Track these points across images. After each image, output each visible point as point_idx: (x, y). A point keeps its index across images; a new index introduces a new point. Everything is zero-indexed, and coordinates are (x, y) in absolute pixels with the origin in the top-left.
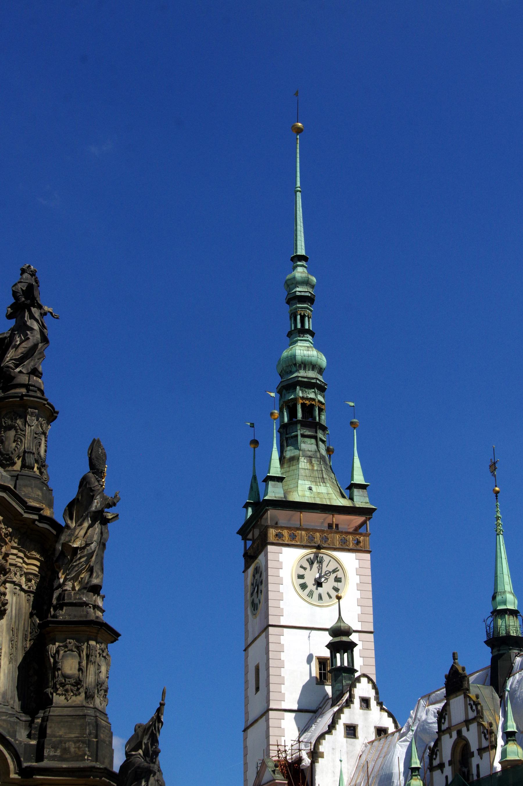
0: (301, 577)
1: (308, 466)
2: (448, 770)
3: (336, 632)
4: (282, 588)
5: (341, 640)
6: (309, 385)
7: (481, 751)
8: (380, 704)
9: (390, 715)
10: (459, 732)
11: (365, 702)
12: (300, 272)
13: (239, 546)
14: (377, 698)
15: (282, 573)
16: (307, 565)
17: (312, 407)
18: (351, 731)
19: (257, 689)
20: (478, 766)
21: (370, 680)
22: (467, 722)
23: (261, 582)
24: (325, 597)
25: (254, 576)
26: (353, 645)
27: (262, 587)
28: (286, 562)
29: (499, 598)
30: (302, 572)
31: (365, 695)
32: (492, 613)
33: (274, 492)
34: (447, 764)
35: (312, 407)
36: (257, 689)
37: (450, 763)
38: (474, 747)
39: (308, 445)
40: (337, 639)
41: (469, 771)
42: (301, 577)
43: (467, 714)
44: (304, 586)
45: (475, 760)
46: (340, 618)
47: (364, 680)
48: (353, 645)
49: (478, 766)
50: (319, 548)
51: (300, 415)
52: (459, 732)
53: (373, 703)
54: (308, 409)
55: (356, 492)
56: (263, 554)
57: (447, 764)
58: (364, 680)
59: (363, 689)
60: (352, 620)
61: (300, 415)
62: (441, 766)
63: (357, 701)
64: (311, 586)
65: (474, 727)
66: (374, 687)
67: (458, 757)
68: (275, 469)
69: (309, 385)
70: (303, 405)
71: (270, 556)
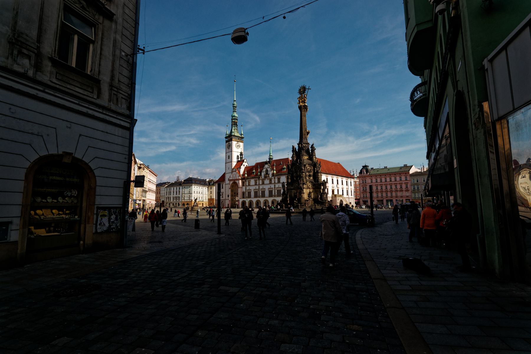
5: (241, 154)
28: (234, 143)
33: (233, 134)
59: (245, 161)
60: (243, 152)
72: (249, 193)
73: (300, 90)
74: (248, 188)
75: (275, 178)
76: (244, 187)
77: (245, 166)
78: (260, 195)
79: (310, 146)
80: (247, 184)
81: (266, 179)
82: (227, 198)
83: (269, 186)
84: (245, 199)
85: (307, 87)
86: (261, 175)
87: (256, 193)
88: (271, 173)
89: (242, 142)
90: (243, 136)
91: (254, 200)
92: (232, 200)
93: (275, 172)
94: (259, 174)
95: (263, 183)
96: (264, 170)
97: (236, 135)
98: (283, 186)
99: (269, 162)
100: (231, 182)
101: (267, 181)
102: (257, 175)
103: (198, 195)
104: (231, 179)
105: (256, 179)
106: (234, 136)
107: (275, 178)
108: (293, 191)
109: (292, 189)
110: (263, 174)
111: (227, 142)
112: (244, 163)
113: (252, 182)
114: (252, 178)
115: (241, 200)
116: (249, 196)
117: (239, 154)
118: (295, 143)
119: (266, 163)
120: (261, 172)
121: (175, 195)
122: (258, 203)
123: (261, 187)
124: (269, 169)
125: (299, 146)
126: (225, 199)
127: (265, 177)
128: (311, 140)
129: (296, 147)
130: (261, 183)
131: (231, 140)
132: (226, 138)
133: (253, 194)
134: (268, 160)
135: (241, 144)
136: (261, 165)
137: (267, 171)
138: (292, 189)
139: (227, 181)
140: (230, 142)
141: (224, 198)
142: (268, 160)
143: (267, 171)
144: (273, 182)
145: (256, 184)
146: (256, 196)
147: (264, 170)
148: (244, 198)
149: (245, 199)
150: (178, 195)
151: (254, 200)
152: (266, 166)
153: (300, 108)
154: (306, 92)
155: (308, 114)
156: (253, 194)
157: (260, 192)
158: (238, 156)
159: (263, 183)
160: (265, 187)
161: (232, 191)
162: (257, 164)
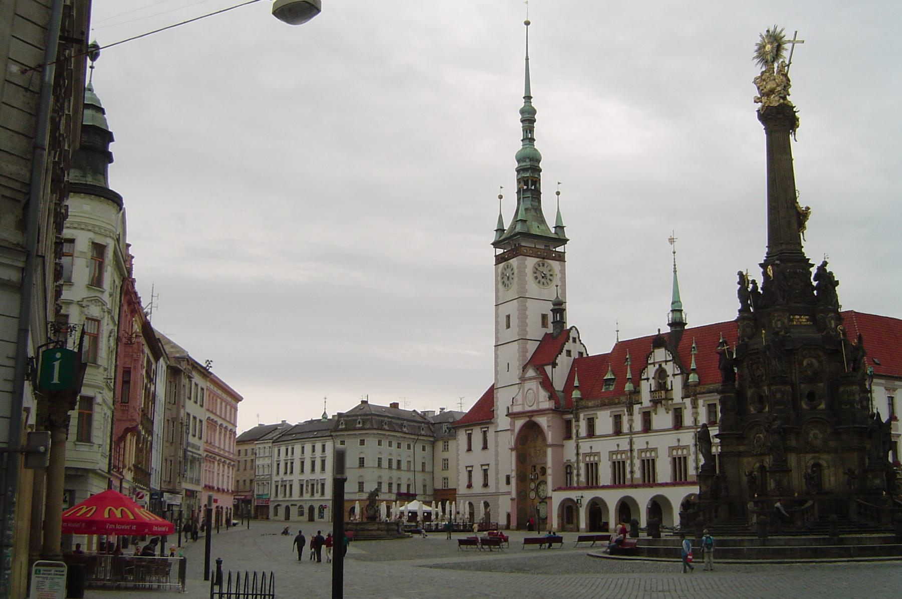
2: (652, 381)
7: (674, 375)
10: (660, 366)
11: (574, 340)
18: (569, 353)
19: (508, 326)
22: (666, 361)
36: (508, 326)
40: (556, 307)
41: (665, 383)
44: (536, 278)
45: (669, 379)
52: (660, 366)
59: (573, 334)
62: (648, 379)
63: (571, 339)
64: (540, 278)
72: (592, 469)
73: (761, 47)
74: (585, 447)
75: (695, 406)
76: (570, 445)
77: (575, 355)
78: (638, 474)
79: (813, 271)
80: (583, 431)
81: (661, 410)
82: (503, 488)
83: (671, 439)
84: (573, 495)
85: (788, 36)
86: (637, 392)
87: (618, 468)
88: (676, 384)
91: (612, 499)
92: (522, 495)
95: (647, 427)
96: (651, 371)
98: (703, 438)
100: (519, 423)
101: (662, 419)
102: (620, 391)
103: (395, 474)
104: (517, 409)
105: (617, 410)
107: (695, 406)
108: (745, 460)
109: (740, 454)
110: (646, 388)
111: (499, 259)
112: (569, 346)
113: (604, 421)
114: (603, 406)
115: (558, 498)
116: (592, 482)
117: (547, 308)
118: (751, 255)
119: (658, 341)
120: (636, 381)
121: (308, 475)
122: (626, 508)
123: (640, 442)
124: (670, 368)
125: (765, 274)
126: (497, 494)
127: (656, 402)
128: (815, 247)
129: (757, 277)
130: (638, 425)
132: (496, 244)
133: (605, 475)
134: (668, 330)
136: (634, 353)
137: (661, 373)
138: (740, 454)
139: (502, 421)
141: (492, 489)
143: (661, 373)
144: (688, 420)
145: (618, 432)
146: (619, 480)
147: (651, 371)
148: (569, 487)
149: (573, 495)
150: (318, 475)
151: (612, 499)
152: (660, 354)
153: (765, 116)
154: (786, 54)
155: (802, 146)
156: (605, 475)
157: (637, 463)
158: (544, 317)
159: (647, 427)
160: (654, 440)
161: (522, 459)
162: (622, 347)
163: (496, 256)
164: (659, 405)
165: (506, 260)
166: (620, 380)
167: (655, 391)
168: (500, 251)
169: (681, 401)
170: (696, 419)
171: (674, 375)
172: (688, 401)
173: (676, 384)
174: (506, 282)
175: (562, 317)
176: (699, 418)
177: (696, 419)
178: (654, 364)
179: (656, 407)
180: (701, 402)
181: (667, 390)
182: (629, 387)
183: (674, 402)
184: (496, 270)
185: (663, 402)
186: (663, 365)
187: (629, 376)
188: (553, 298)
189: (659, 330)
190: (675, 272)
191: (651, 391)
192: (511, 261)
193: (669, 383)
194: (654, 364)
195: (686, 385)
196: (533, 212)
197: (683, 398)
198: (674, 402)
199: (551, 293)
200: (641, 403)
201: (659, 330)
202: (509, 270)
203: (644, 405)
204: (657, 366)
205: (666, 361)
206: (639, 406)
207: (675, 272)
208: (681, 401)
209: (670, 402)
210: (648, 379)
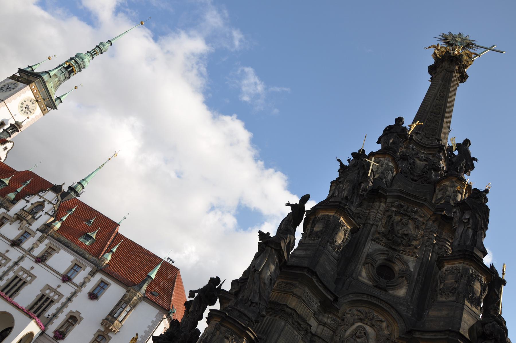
0: (25, 101)
1: (57, 82)
2: (29, 205)
3: (17, 123)
4: (18, 98)
5: (15, 127)
6: (79, 67)
7: (46, 213)
8: (8, 152)
9: (6, 157)
10: (44, 201)
12: (107, 45)
13: (15, 71)
14: (9, 151)
15: (23, 95)
16: (29, 100)
17: (74, 72)
20: (41, 215)
21: (13, 145)
22: (50, 202)
23: (13, 89)
24: (23, 111)
25: (11, 84)
26: (18, 131)
27: (12, 91)
28: (27, 93)
29: (84, 182)
30: (26, 100)
31: (8, 147)
32: (78, 183)
33: (45, 77)
34: (30, 203)
35: (74, 72)
37: (32, 204)
38: (46, 209)
39: (62, 78)
40: (16, 125)
42: (25, 101)
43: (52, 200)
44: (22, 104)
45: (41, 213)
46: (22, 122)
47: (12, 143)
48: (18, 131)
49: (41, 215)
50: (37, 101)
51: (69, 70)
52: (44, 201)
53: (7, 151)
54: (72, 71)
55: (58, 101)
56: (24, 84)
57: (30, 203)
58: (12, 143)
59: (9, 145)
61: (69, 70)
62: (28, 201)
63: (4, 146)
64: (24, 106)
65: (51, 206)
66: (12, 148)
67: (36, 205)
68: (52, 74)
69: (79, 67)
70: (73, 69)
71: (26, 88)
75: (40, 240)
81: (16, 224)
86: (14, 202)
88: (43, 218)
89: (44, 112)
90: (56, 103)
93: (58, 225)
94: (12, 196)
96: (35, 199)
97: (49, 85)
99: (64, 195)
106: (44, 83)
107: (40, 240)
110: (21, 204)
119: (57, 189)
124: (48, 207)
127: (19, 217)
131: (28, 83)
132: (20, 71)
135: (38, 111)
137: (40, 206)
140: (21, 85)
142: (65, 189)
143: (40, 206)
144: (27, 245)
152: (50, 196)
162: (29, 174)
163: (14, 75)
164: (18, 221)
165: (18, 81)
166: (10, 189)
167: (25, 211)
168: (18, 75)
169: (35, 230)
170: (32, 248)
171: (46, 213)
172: (39, 234)
173: (43, 218)
174: (5, 88)
175: (12, 133)
176: (36, 250)
177: (32, 248)
178: (41, 197)
179: (15, 221)
180: (47, 241)
181: (33, 217)
182: (12, 196)
183: (31, 227)
184: (6, 80)
185: (24, 222)
186: (46, 203)
187: (19, 190)
188: (19, 120)
189: (64, 184)
190: (100, 167)
191: (23, 209)
192: (20, 83)
193: (38, 215)
194: (41, 197)
195: (48, 226)
196: (57, 80)
197: (38, 230)
198: (31, 227)
199: (20, 118)
200: (9, 211)
201: (64, 184)
202: (14, 86)
203: (9, 213)
204: (42, 200)
205: (50, 202)
206: (5, 211)
207: (100, 167)
208: (35, 230)
209: (27, 225)
210: (28, 201)
